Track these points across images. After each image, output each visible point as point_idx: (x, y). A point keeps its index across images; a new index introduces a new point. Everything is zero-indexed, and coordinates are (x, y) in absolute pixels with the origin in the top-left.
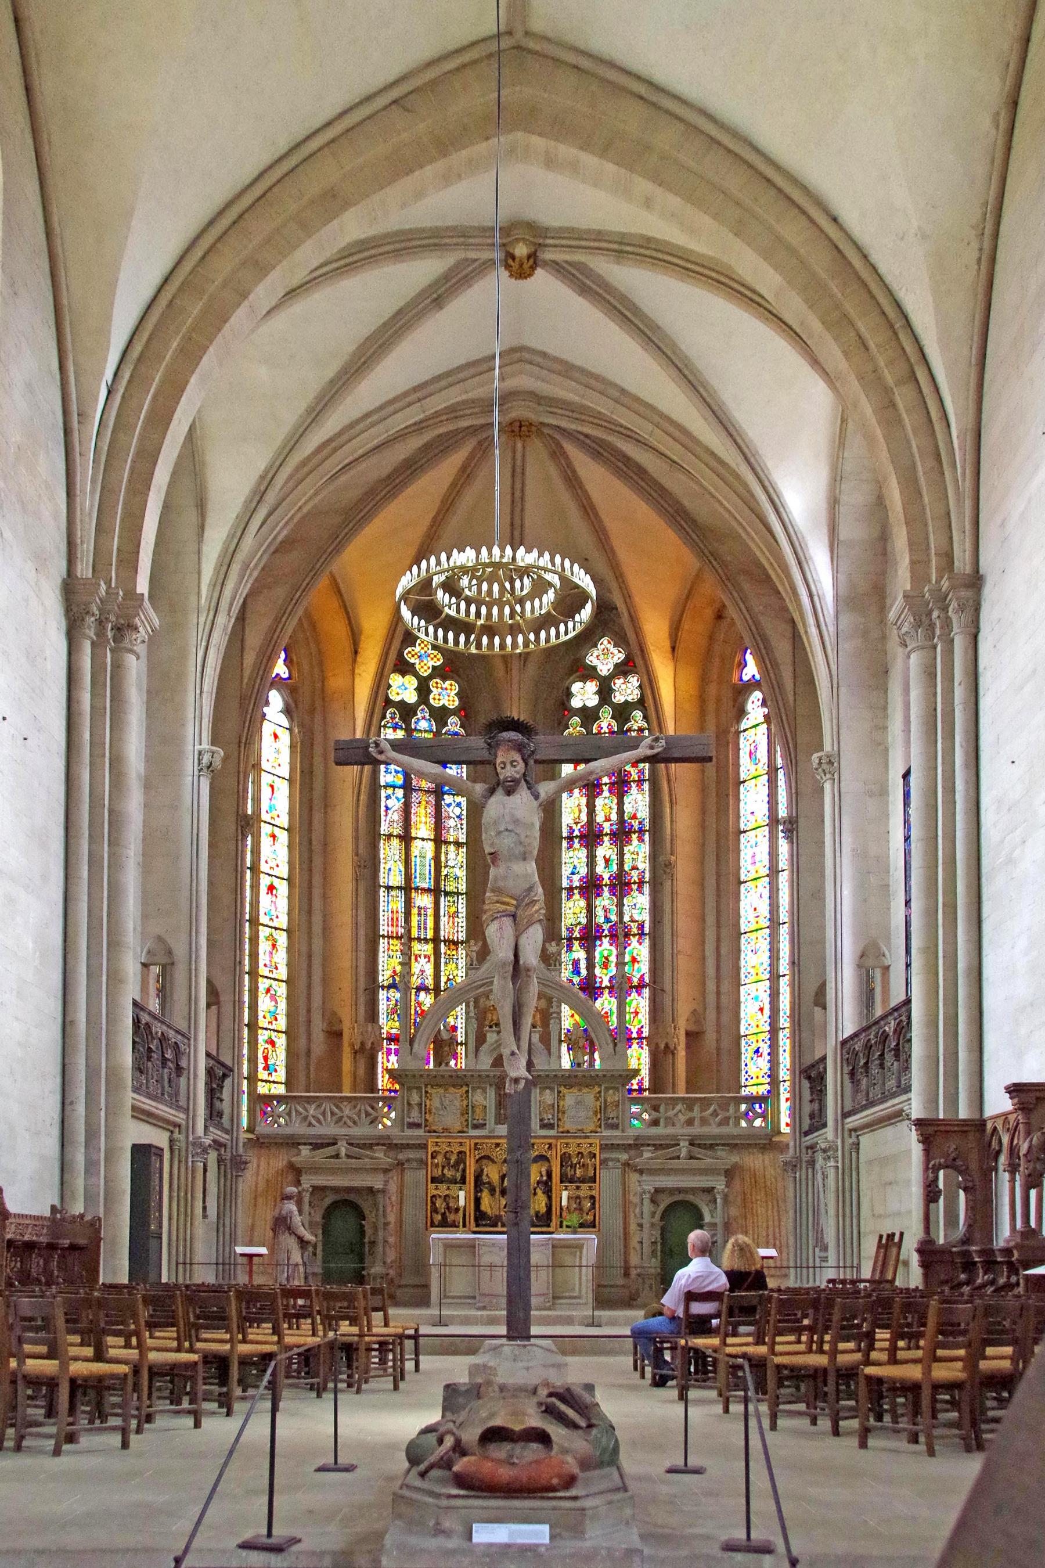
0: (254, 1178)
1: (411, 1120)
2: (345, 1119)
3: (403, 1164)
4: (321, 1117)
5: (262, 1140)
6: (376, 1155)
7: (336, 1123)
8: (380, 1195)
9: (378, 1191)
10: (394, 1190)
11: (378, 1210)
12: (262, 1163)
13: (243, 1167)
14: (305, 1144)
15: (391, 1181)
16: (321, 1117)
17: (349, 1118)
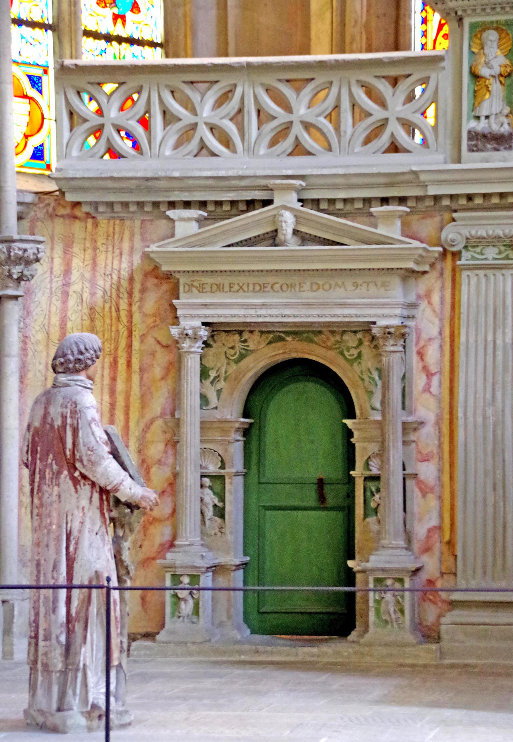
0: (57, 304)
1: (481, 126)
2: (297, 130)
3: (457, 255)
4: (231, 128)
5: (70, 197)
6: (382, 230)
7: (273, 143)
8: (390, 345)
9: (387, 333)
10: (434, 331)
11: (386, 387)
12: (76, 263)
13: (16, 271)
14: (187, 205)
15: (423, 304)
16: (231, 128)
17: (307, 126)
